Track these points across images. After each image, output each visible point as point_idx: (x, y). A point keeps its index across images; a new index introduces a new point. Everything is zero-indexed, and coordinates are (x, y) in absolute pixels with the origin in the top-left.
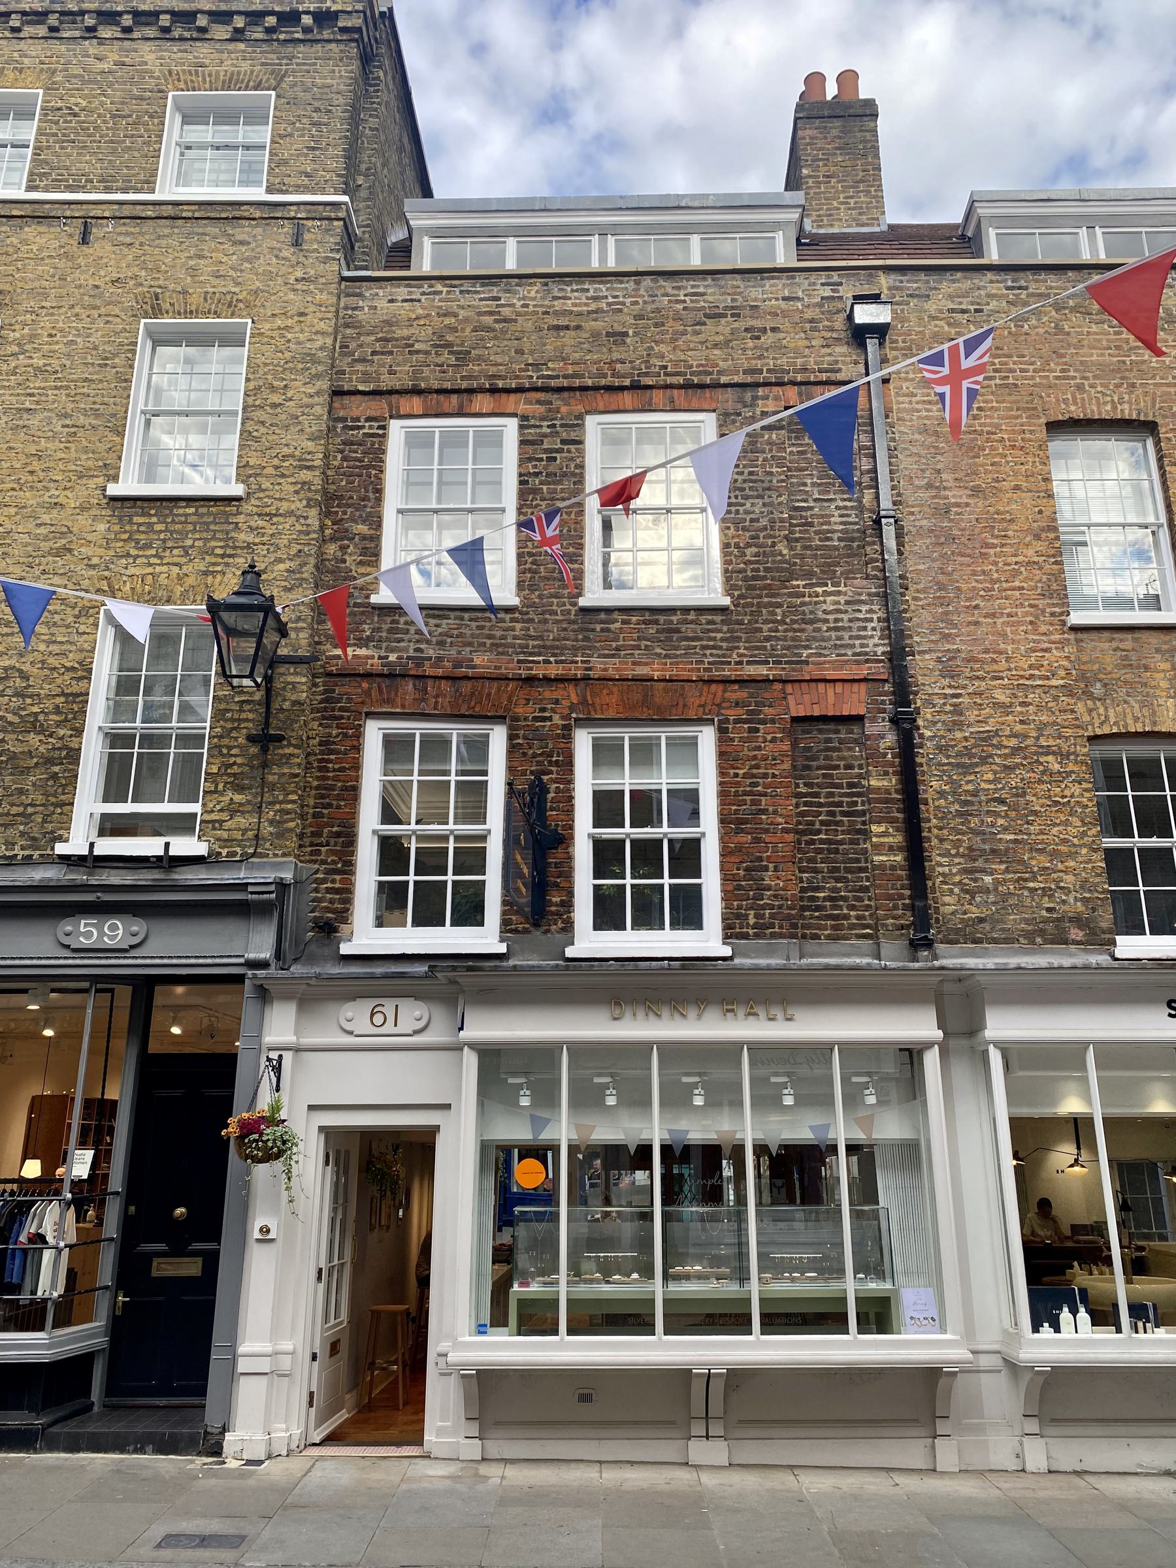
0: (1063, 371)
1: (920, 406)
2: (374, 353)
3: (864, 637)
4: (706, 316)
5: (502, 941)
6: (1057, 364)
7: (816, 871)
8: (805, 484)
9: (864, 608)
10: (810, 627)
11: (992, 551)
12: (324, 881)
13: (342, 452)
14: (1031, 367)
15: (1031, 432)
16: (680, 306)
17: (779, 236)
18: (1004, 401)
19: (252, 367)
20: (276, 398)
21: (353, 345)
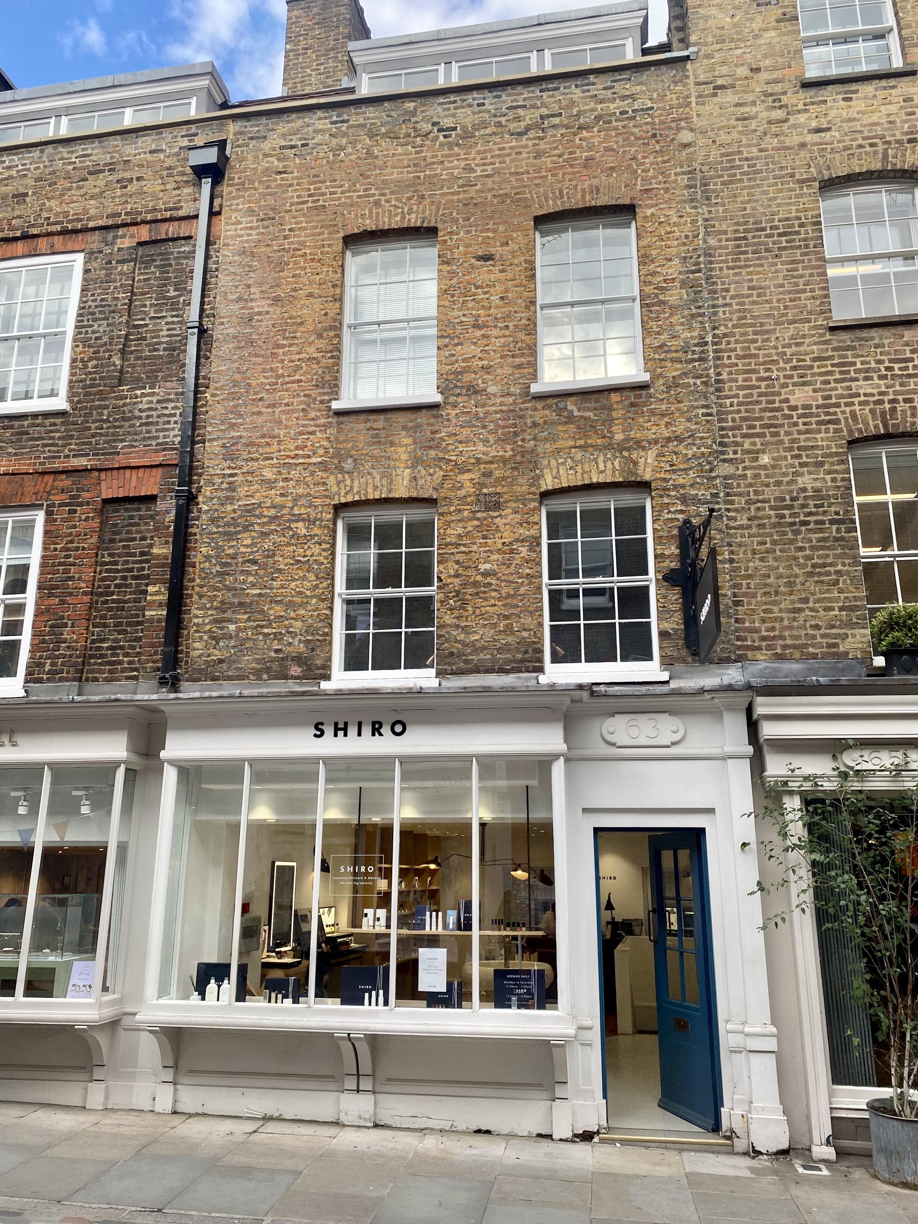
1: (243, 232)
7: (105, 626)
8: (145, 306)
9: (171, 405)
10: (127, 424)
11: (281, 351)
15: (329, 246)
17: (194, 101)
18: (312, 221)
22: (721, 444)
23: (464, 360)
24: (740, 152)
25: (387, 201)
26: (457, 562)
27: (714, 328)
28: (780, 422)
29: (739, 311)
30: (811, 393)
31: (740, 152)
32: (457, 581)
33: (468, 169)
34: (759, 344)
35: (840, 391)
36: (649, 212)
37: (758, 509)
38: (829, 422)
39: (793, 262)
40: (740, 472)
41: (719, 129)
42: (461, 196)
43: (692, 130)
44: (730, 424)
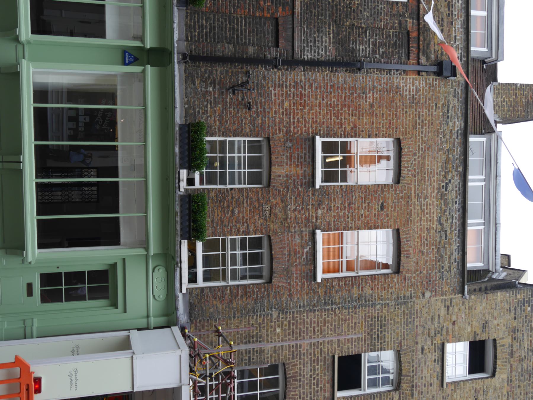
0: (422, 148)
1: (408, 87)
3: (311, 52)
6: (425, 147)
8: (376, 36)
9: (323, 53)
11: (346, 109)
14: (424, 136)
15: (396, 131)
17: (486, 50)
18: (409, 122)
22: (287, 312)
23: (334, 199)
24: (417, 317)
25: (415, 159)
26: (239, 198)
27: (339, 308)
28: (295, 336)
29: (346, 319)
30: (306, 348)
31: (417, 317)
32: (230, 198)
33: (426, 197)
34: (330, 327)
35: (306, 359)
36: (395, 280)
37: (257, 328)
38: (293, 355)
39: (365, 340)
40: (273, 320)
41: (429, 309)
42: (413, 195)
43: (430, 297)
44: (295, 316)
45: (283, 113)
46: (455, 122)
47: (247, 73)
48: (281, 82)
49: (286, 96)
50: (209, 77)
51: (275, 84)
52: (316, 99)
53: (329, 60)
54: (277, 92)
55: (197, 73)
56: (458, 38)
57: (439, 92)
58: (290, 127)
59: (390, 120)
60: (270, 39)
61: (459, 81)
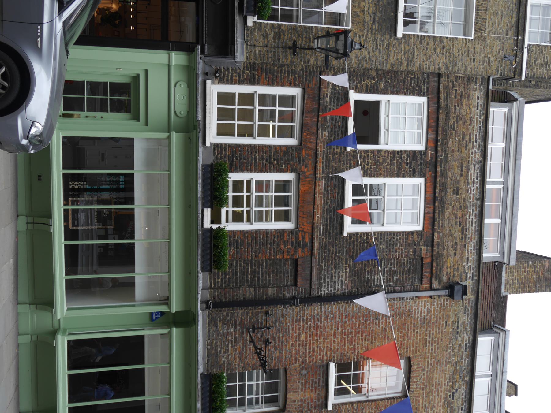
0: (431, 363)
1: (420, 310)
2: (456, 90)
3: (328, 287)
4: (463, 227)
5: (211, 144)
6: (434, 362)
7: (236, 266)
8: (391, 265)
9: (339, 287)
10: (333, 266)
11: (360, 335)
12: (236, 73)
13: (414, 77)
14: (433, 352)
15: (407, 351)
16: (467, 216)
17: (498, 255)
19: (452, 39)
20: (438, 50)
21: (460, 81)
25: (424, 374)
45: (299, 345)
46: (464, 337)
47: (267, 313)
48: (298, 317)
49: (303, 329)
50: (231, 319)
51: (293, 320)
52: (332, 329)
53: (345, 293)
54: (294, 326)
55: (220, 317)
56: (470, 259)
57: (450, 311)
58: (306, 357)
59: (401, 341)
60: (289, 278)
61: (469, 299)
